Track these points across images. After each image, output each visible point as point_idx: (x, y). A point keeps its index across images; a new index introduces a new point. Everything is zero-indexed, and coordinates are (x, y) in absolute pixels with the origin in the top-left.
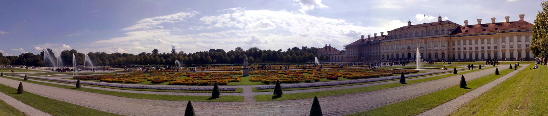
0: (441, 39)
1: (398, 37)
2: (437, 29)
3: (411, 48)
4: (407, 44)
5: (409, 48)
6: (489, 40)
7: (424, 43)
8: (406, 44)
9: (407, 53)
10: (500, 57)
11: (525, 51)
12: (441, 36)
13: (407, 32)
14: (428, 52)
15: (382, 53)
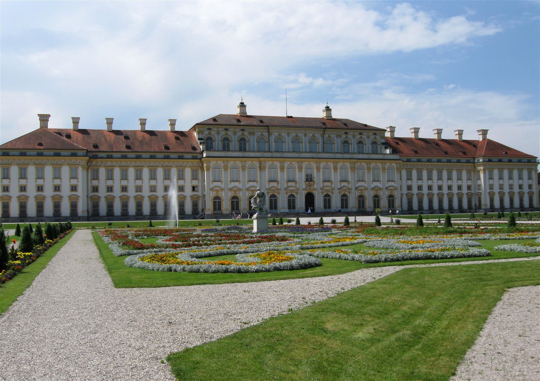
0: (373, 165)
1: (234, 144)
2: (347, 137)
3: (315, 180)
4: (303, 170)
5: (309, 179)
6: (459, 172)
7: (350, 171)
8: (300, 168)
9: (304, 193)
10: (486, 205)
11: (499, 195)
12: (320, 155)
13: (266, 134)
14: (358, 193)
15: (212, 189)
